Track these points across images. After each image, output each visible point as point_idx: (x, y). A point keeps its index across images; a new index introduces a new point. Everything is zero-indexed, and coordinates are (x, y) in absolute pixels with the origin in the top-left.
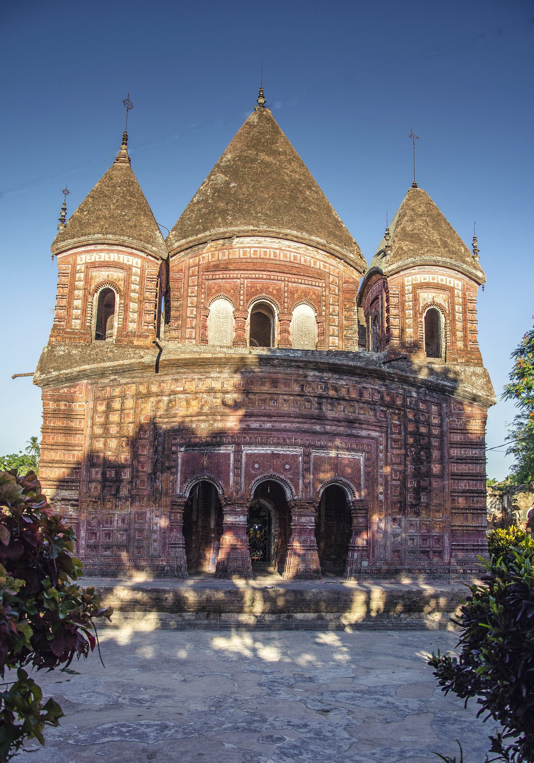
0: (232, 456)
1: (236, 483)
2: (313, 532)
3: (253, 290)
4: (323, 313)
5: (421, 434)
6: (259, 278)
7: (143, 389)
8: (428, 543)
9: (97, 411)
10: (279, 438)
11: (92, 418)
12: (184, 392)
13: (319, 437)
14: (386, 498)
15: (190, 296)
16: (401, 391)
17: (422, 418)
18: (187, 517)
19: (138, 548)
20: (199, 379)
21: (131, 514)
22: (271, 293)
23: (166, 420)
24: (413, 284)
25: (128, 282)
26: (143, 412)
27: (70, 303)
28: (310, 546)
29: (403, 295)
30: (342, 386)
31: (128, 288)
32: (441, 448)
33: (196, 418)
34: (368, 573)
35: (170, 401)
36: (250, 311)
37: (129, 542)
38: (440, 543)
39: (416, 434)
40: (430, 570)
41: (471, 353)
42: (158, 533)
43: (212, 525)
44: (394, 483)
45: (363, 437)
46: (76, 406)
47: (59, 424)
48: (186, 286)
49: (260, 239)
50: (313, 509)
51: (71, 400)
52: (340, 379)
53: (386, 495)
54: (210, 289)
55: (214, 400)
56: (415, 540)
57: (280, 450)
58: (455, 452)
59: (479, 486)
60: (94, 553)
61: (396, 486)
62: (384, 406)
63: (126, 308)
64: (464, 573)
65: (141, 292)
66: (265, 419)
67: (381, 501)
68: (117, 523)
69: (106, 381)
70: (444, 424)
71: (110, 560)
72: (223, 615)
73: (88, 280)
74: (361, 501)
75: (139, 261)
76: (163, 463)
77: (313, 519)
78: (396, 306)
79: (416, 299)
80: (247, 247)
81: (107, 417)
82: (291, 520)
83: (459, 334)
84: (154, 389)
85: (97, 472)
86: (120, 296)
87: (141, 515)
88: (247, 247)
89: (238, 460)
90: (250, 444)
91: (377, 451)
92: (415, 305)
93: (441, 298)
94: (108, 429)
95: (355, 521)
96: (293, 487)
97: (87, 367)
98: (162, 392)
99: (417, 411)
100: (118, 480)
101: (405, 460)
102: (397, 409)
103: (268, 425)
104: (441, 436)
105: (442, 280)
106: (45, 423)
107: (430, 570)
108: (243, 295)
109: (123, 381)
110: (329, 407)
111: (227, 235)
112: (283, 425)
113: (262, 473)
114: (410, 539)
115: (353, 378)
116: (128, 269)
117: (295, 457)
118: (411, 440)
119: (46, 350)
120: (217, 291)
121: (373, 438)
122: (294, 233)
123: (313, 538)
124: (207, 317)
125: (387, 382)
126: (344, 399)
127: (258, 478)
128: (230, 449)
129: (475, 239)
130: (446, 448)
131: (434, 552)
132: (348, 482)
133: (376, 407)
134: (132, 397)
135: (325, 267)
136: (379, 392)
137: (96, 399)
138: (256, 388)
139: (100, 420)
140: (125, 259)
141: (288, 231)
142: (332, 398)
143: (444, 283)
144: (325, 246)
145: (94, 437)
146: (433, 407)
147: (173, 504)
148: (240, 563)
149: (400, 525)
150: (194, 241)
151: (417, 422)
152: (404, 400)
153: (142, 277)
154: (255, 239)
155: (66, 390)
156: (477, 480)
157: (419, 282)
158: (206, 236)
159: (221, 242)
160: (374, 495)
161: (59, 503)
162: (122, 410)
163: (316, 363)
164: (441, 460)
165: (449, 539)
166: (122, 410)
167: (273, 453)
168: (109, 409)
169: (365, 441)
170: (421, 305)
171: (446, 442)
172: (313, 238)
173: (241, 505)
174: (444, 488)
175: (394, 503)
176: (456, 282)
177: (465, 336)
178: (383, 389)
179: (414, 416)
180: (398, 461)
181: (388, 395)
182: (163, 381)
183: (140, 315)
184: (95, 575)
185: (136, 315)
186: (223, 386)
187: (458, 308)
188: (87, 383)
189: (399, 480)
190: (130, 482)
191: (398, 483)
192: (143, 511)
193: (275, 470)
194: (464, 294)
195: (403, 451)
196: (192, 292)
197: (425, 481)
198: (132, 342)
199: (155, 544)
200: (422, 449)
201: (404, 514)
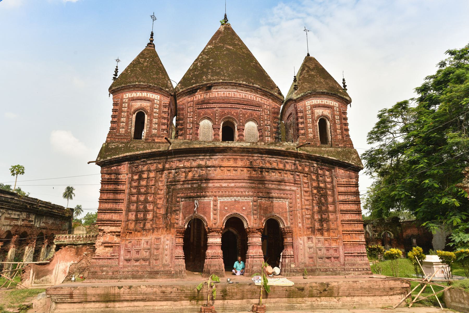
0: (212, 203)
2: (261, 247)
5: (321, 188)
11: (130, 183)
12: (184, 167)
14: (303, 225)
16: (307, 164)
18: (186, 240)
23: (173, 183)
24: (310, 105)
29: (306, 111)
30: (274, 162)
33: (191, 182)
39: (318, 188)
43: (202, 243)
44: (307, 216)
46: (121, 177)
47: (111, 187)
50: (260, 233)
52: (272, 158)
53: (303, 223)
55: (201, 171)
58: (341, 198)
61: (308, 219)
66: (231, 181)
69: (138, 161)
74: (289, 227)
76: (171, 208)
77: (260, 239)
78: (302, 118)
81: (139, 183)
82: (247, 241)
83: (339, 131)
90: (222, 196)
93: (327, 112)
94: (140, 189)
95: (285, 241)
98: (171, 167)
99: (318, 175)
103: (232, 185)
104: (333, 189)
109: (149, 162)
110: (267, 173)
112: (241, 184)
115: (280, 157)
118: (315, 191)
119: (104, 145)
121: (293, 191)
126: (275, 169)
130: (336, 196)
137: (133, 173)
139: (134, 184)
142: (268, 169)
145: (131, 194)
147: (178, 232)
151: (318, 181)
155: (115, 168)
160: (295, 224)
162: (148, 178)
163: (258, 149)
164: (334, 203)
169: (288, 192)
170: (316, 116)
173: (218, 232)
174: (337, 218)
177: (342, 132)
178: (297, 162)
179: (316, 177)
182: (172, 161)
186: (206, 163)
187: (337, 117)
188: (128, 163)
190: (153, 220)
193: (237, 210)
194: (340, 109)
195: (311, 198)
197: (325, 214)
201: (314, 235)
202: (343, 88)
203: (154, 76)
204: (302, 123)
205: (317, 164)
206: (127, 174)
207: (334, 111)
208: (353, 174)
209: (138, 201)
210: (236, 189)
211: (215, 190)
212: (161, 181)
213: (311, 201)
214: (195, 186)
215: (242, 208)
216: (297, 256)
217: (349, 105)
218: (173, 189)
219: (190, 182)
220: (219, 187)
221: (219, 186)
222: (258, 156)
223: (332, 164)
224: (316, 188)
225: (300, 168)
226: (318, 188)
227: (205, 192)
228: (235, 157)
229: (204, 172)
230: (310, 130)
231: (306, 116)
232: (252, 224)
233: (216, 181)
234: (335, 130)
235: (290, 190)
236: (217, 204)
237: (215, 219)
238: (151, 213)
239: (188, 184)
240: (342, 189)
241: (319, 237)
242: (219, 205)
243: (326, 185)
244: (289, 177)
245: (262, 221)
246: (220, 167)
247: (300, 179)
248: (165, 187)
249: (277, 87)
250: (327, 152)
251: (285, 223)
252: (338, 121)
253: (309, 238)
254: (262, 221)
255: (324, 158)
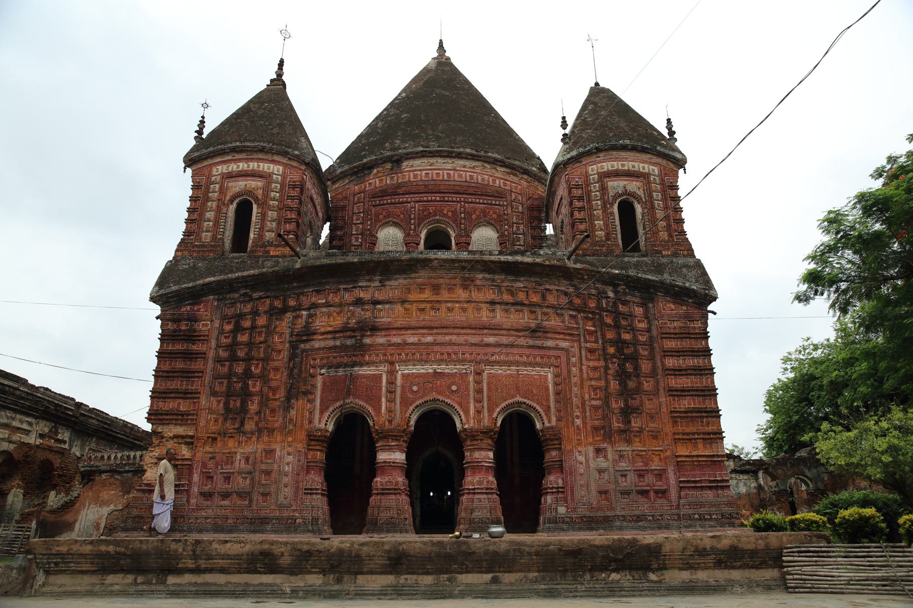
1: (390, 411)
3: (425, 213)
4: (506, 233)
5: (624, 342)
6: (431, 201)
7: (278, 304)
8: (646, 480)
9: (223, 330)
10: (442, 354)
13: (491, 350)
14: (584, 423)
15: (355, 224)
16: (594, 292)
17: (624, 323)
19: (265, 495)
20: (345, 289)
21: (256, 452)
22: (445, 215)
24: (598, 173)
25: (267, 189)
26: (277, 330)
27: (201, 215)
28: (487, 489)
29: (588, 185)
30: (519, 289)
31: (266, 196)
32: (652, 358)
34: (567, 523)
35: (310, 316)
36: (423, 235)
37: (253, 487)
38: (664, 480)
39: (619, 343)
40: (653, 516)
41: (678, 244)
42: (290, 475)
45: (549, 348)
47: (179, 347)
48: (350, 213)
49: (432, 160)
50: (490, 441)
51: (193, 319)
52: (516, 280)
54: (377, 215)
56: (628, 477)
57: (442, 368)
58: (670, 362)
59: (708, 405)
60: (209, 503)
61: (596, 408)
62: (573, 310)
63: (263, 217)
64: (700, 519)
65: (280, 200)
66: (425, 331)
67: (578, 428)
68: (239, 463)
69: (236, 295)
70: (654, 328)
71: (228, 512)
72: (359, 577)
73: (222, 191)
74: (552, 428)
75: (281, 168)
77: (491, 454)
78: (580, 198)
79: (604, 189)
80: (418, 170)
81: (235, 337)
82: (463, 457)
84: (292, 303)
85: (219, 402)
86: (259, 206)
87: (270, 453)
88: (418, 170)
89: (391, 382)
90: (406, 362)
91: (568, 364)
92: (603, 195)
93: (634, 186)
95: (547, 457)
96: (461, 413)
97: (212, 279)
98: (300, 305)
99: (617, 315)
100: (244, 410)
101: (606, 374)
102: (591, 313)
103: (429, 339)
105: (633, 167)
106: (161, 346)
107: (653, 516)
108: (414, 219)
109: (256, 295)
111: (395, 158)
112: (447, 338)
113: (421, 397)
114: (622, 476)
115: (532, 279)
116: (265, 177)
117: (463, 376)
118: (612, 350)
120: (385, 217)
121: (562, 349)
122: (468, 150)
123: (491, 478)
124: (375, 245)
125: (576, 282)
126: (522, 304)
127: (418, 403)
128: (383, 369)
129: (669, 121)
130: (658, 358)
131: (657, 492)
132: (535, 405)
133: (563, 312)
134: (265, 312)
135: (505, 184)
136: (566, 294)
137: (224, 318)
138: (411, 297)
139: (224, 340)
140: (265, 167)
141: (462, 150)
142: (507, 304)
143: (636, 169)
144: (504, 162)
145: (218, 360)
146: (636, 308)
148: (393, 513)
149: (605, 457)
150: (359, 166)
151: (617, 326)
152: (599, 302)
153: (283, 185)
154: (425, 160)
156: (704, 396)
157: (605, 170)
158: (372, 160)
159: (389, 166)
160: (567, 420)
161: (171, 442)
162: (253, 327)
164: (653, 373)
165: (675, 474)
166: (253, 327)
167: (435, 373)
168: (238, 329)
169: (552, 353)
170: (611, 194)
171: (657, 350)
172: (490, 154)
173: (396, 438)
175: (596, 429)
176: (651, 167)
177: (669, 225)
178: (571, 290)
180: (597, 375)
181: (577, 297)
182: (302, 293)
183: (279, 224)
184: (207, 531)
185: (274, 224)
189: (599, 399)
190: (258, 413)
191: (598, 403)
192: (273, 447)
193: (439, 393)
195: (602, 363)
196: (357, 220)
197: (635, 399)
198: (268, 252)
199: (286, 490)
200: (627, 359)
202: (668, 137)
203: (274, 131)
204: (581, 209)
205: (616, 292)
206: (212, 321)
207: (649, 182)
208: (696, 312)
209: (230, 375)
210: (436, 348)
211: (390, 350)
212: (281, 335)
213: (602, 370)
214: (349, 342)
215: (449, 387)
216: (572, 491)
217: (681, 171)
218: (303, 351)
219: (337, 335)
220: (399, 345)
221: (399, 341)
222: (484, 278)
223: (647, 291)
224: (613, 342)
225: (577, 301)
226: (619, 343)
227: (370, 355)
228: (435, 282)
229: (368, 314)
230: (599, 223)
231: (589, 196)
232: (472, 421)
233: (394, 332)
234: (654, 221)
235: (554, 348)
236: (396, 378)
237: (392, 412)
238: (256, 400)
239: (335, 338)
240: (671, 344)
241: (624, 447)
242: (399, 381)
243: (635, 336)
244: (553, 322)
245: (495, 415)
246: (403, 302)
247: (577, 323)
248: (287, 345)
249: (539, 158)
250: (636, 267)
251: (545, 418)
252: (658, 204)
253: (598, 451)
254: (495, 415)
255: (628, 276)
